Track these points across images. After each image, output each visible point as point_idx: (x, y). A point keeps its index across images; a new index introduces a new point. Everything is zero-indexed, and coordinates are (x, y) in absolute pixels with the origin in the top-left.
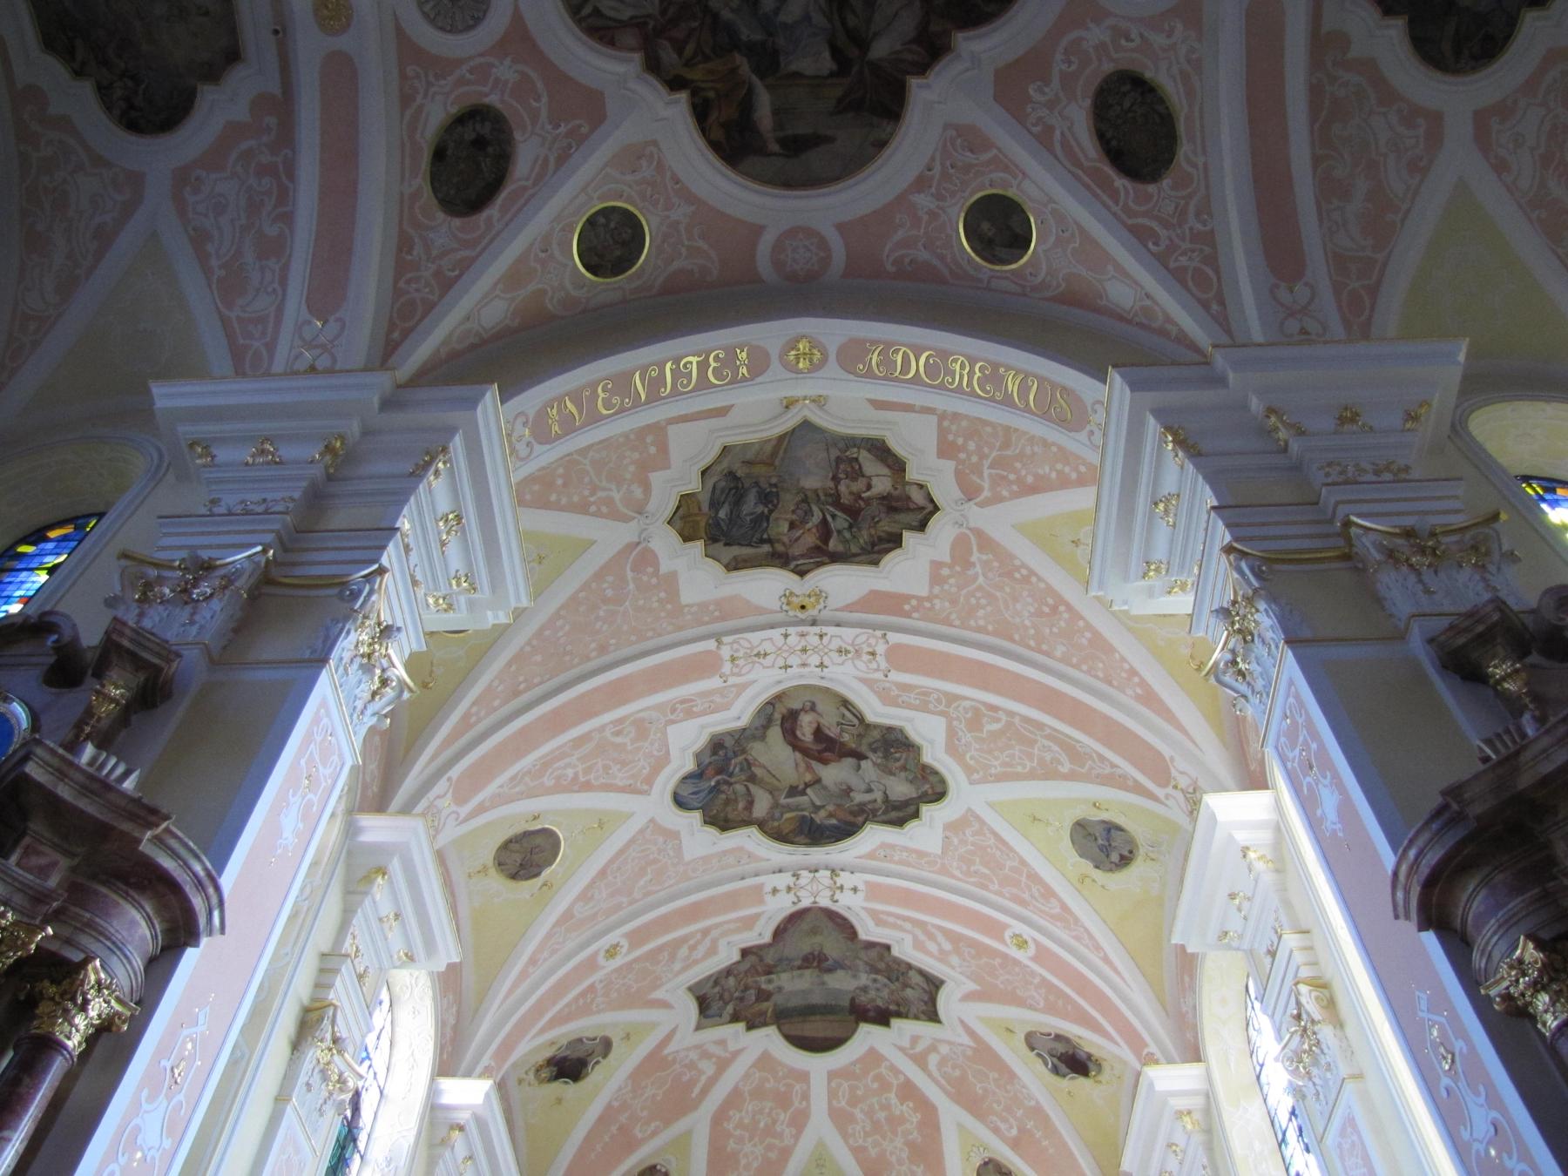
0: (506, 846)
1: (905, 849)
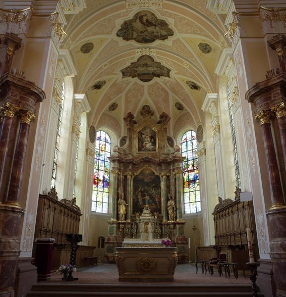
0: (82, 47)
1: (164, 45)
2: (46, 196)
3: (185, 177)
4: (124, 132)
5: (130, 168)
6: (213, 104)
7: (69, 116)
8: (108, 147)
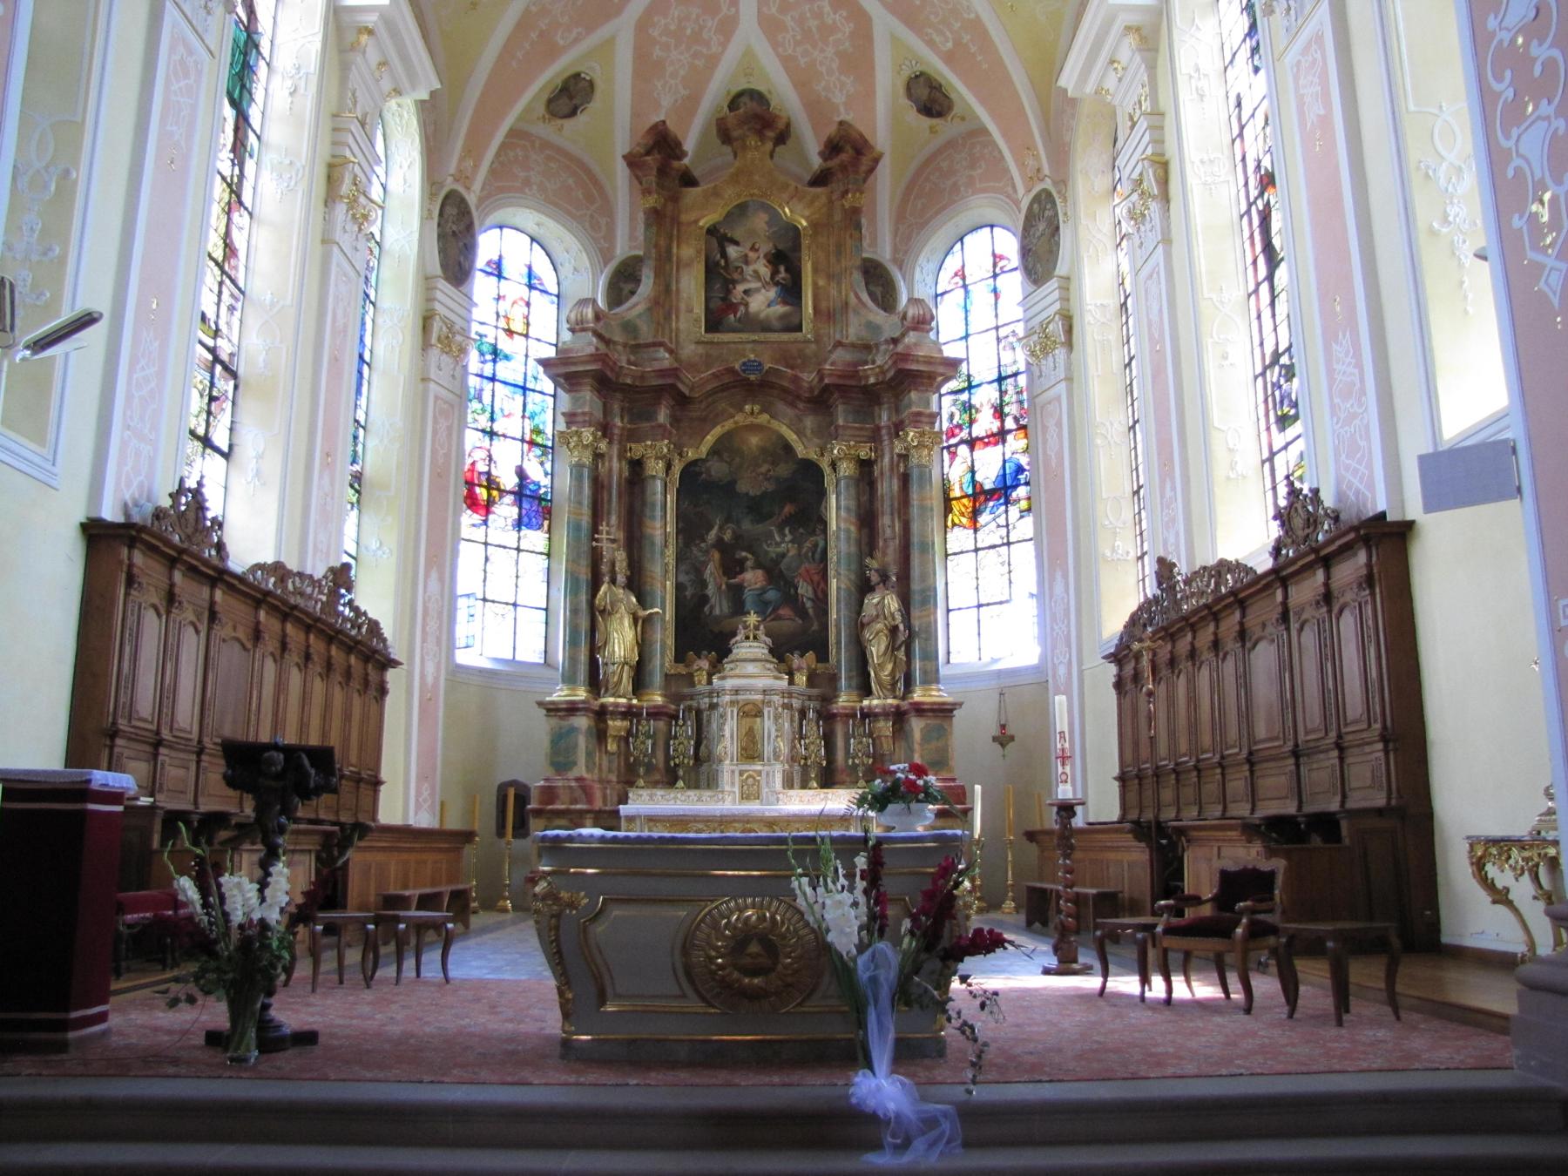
2: (141, 529)
3: (956, 472)
4: (627, 240)
5: (663, 416)
6: (1131, 41)
7: (308, 103)
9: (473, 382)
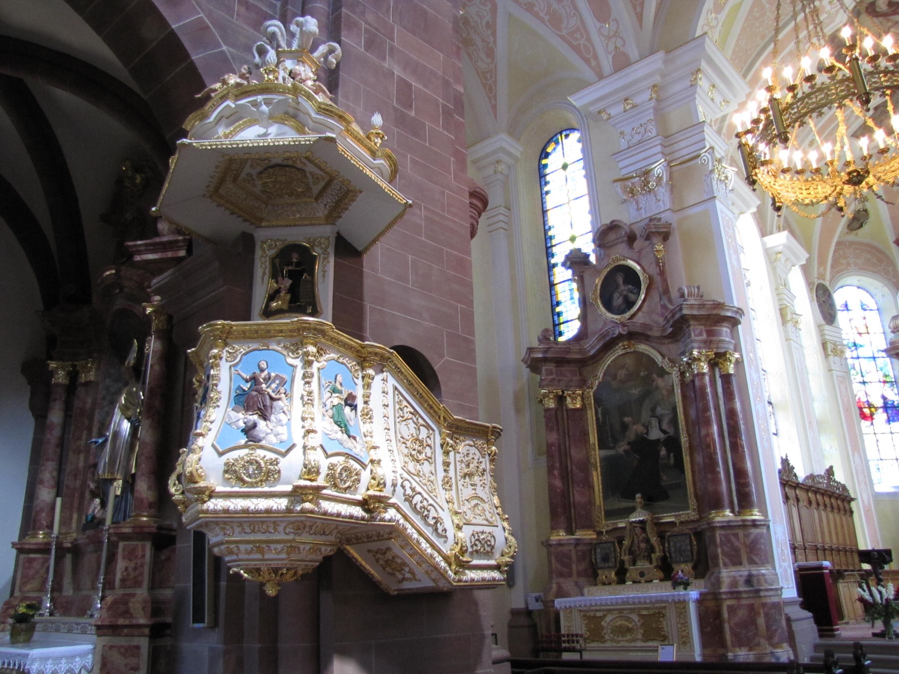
8: (874, 319)
9: (850, 362)
